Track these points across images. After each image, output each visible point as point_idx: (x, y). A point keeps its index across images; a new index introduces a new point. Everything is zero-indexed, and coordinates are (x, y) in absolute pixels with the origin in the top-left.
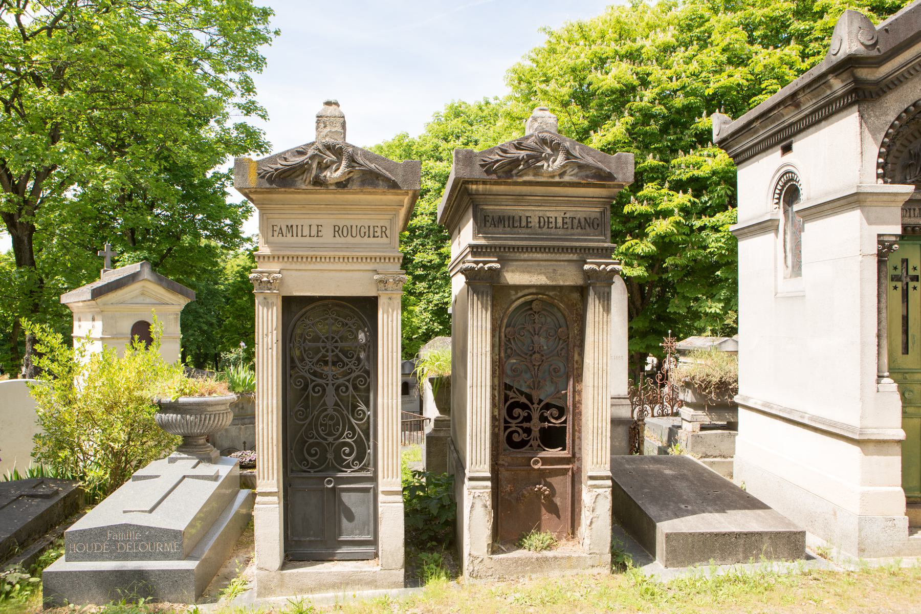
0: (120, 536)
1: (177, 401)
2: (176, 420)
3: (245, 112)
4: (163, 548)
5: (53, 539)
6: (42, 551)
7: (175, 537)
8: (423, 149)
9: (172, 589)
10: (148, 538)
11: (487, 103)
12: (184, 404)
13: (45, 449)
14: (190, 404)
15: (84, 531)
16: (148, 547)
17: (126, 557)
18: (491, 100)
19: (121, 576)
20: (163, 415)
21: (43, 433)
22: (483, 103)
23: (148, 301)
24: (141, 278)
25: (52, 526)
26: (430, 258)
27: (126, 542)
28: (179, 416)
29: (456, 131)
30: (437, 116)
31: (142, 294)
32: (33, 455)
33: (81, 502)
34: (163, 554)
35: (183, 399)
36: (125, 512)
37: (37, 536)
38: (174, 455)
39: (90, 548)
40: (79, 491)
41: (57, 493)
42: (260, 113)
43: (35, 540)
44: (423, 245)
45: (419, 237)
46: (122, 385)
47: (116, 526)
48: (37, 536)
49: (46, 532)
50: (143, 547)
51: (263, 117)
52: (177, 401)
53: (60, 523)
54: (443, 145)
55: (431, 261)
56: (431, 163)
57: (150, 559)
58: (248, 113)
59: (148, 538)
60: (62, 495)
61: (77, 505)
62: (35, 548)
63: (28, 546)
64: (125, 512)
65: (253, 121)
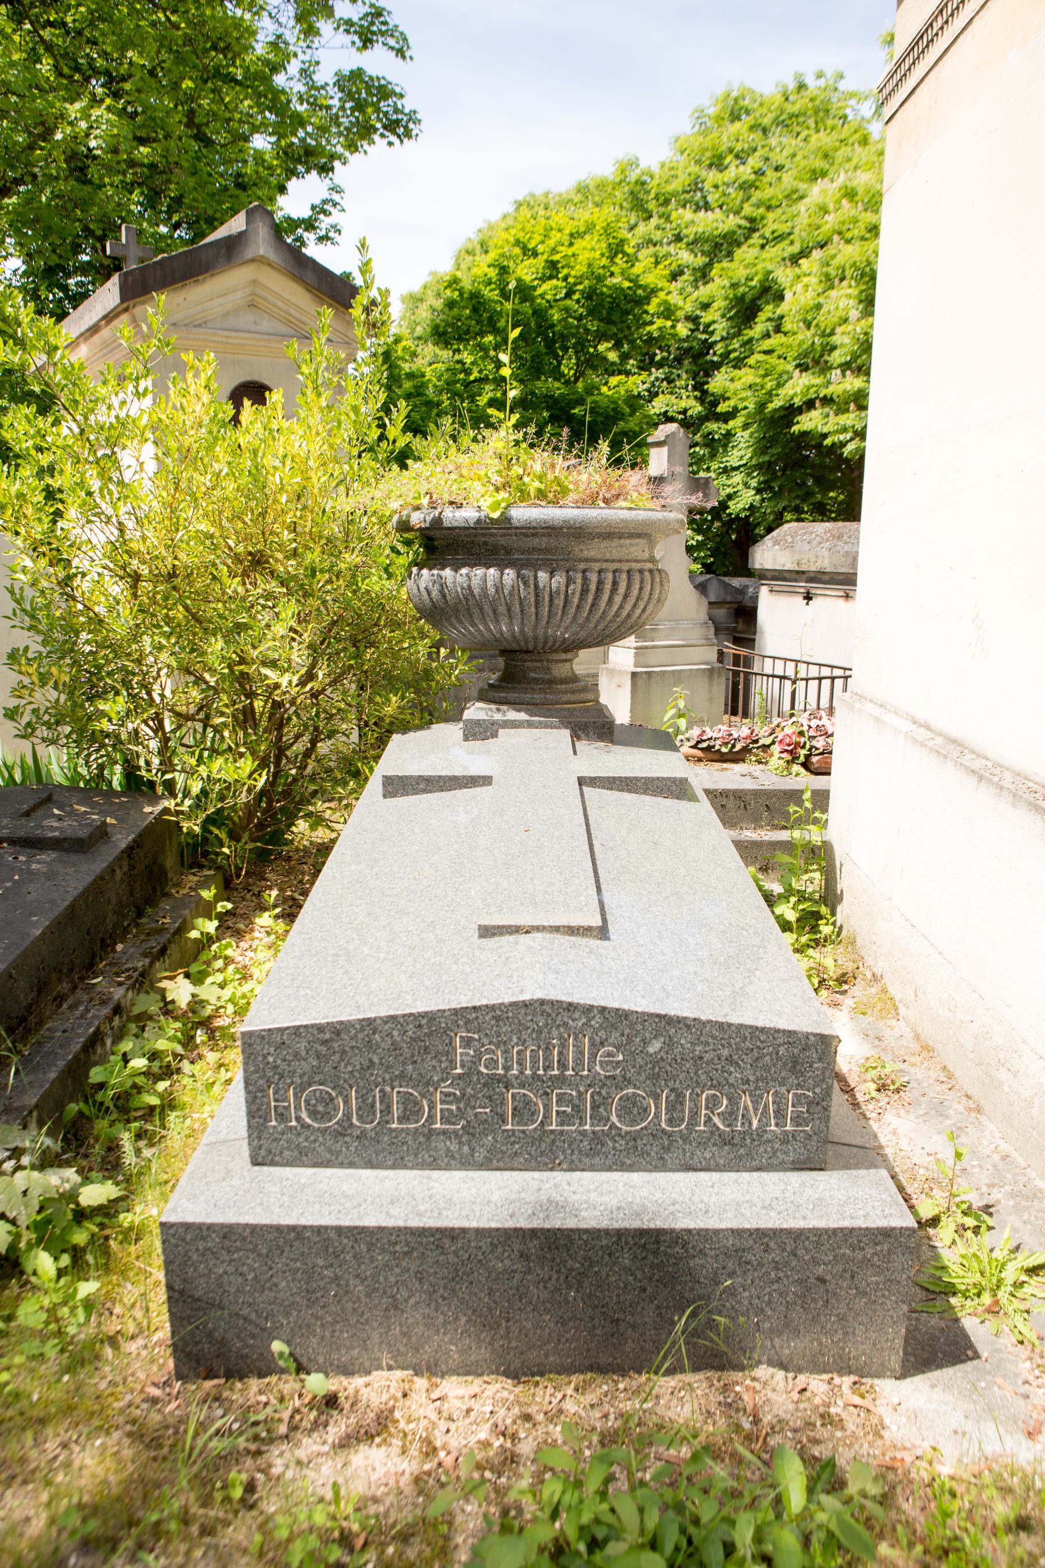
0: (518, 1060)
1: (505, 519)
2: (499, 587)
3: (359, 44)
4: (729, 1117)
5: (118, 993)
6: (93, 1047)
7: (795, 1065)
8: (670, 188)
9: (797, 1314)
10: (656, 1073)
11: (801, 87)
12: (531, 530)
13: (46, 696)
14: (551, 530)
15: (338, 1029)
16: (658, 1112)
17: (545, 1152)
18: (811, 82)
19: (553, 1252)
20: (448, 573)
21: (34, 644)
22: (792, 85)
23: (266, 325)
24: (249, 254)
25: (106, 945)
26: (683, 404)
27: (543, 1085)
28: (510, 575)
29: (739, 147)
30: (699, 115)
31: (252, 305)
32: (12, 714)
33: (170, 861)
34: (727, 1141)
35: (521, 514)
36: (487, 932)
37: (65, 986)
38: (476, 711)
39: (366, 1109)
40: (164, 828)
41: (102, 833)
42: (392, 42)
43: (61, 999)
44: (670, 381)
45: (660, 365)
46: (280, 478)
47: (498, 1013)
48: (65, 986)
49: (90, 968)
50: (632, 1109)
51: (400, 53)
52: (505, 519)
53: (126, 931)
54: (712, 177)
55: (684, 412)
56: (688, 214)
57: (661, 1166)
58: (367, 42)
59: (656, 1073)
60: (123, 840)
61: (163, 872)
62: (68, 1028)
63: (40, 1024)
64: (487, 932)
65: (377, 62)
